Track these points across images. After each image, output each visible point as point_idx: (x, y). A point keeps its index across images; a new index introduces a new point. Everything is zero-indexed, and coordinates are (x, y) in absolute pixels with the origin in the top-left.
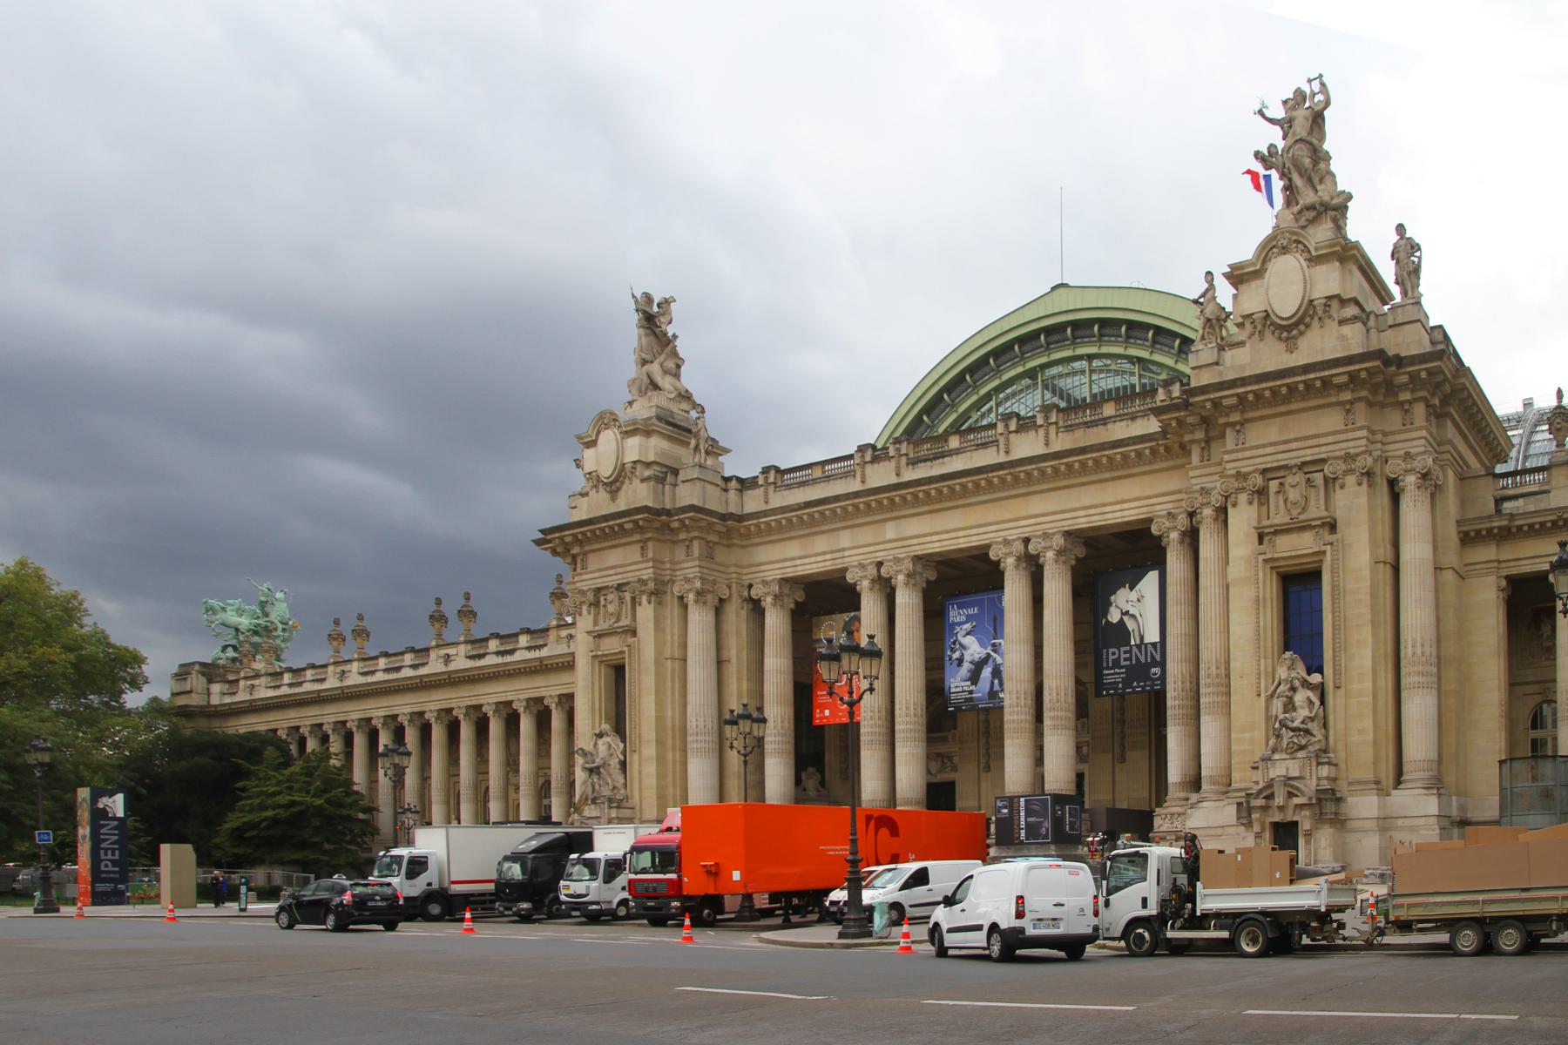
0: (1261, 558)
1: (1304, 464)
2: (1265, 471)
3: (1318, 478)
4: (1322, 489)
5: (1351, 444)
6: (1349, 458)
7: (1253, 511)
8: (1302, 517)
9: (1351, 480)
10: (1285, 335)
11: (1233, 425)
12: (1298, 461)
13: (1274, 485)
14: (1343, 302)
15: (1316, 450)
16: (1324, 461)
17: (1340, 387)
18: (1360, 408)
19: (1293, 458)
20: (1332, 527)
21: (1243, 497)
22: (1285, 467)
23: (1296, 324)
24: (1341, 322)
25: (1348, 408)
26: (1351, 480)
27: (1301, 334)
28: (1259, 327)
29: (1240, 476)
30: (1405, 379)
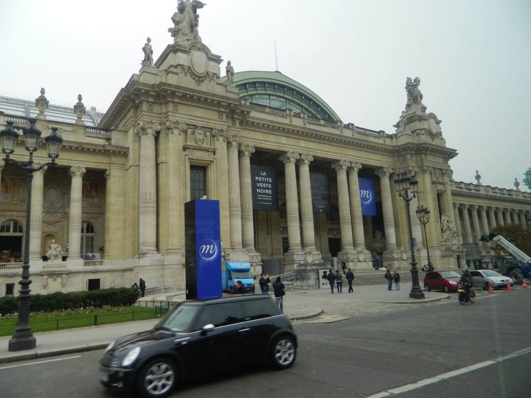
0: (187, 157)
1: (203, 127)
2: (187, 124)
3: (208, 134)
4: (209, 139)
5: (216, 125)
6: (222, 131)
7: (182, 137)
8: (203, 146)
9: (221, 139)
10: (197, 78)
11: (174, 103)
12: (200, 125)
13: (190, 131)
15: (207, 123)
16: (212, 129)
17: (223, 106)
18: (224, 116)
19: (199, 124)
20: (214, 153)
21: (176, 132)
22: (195, 126)
23: (201, 77)
25: (220, 113)
26: (221, 139)
27: (203, 81)
28: (186, 71)
29: (177, 123)
30: (239, 111)
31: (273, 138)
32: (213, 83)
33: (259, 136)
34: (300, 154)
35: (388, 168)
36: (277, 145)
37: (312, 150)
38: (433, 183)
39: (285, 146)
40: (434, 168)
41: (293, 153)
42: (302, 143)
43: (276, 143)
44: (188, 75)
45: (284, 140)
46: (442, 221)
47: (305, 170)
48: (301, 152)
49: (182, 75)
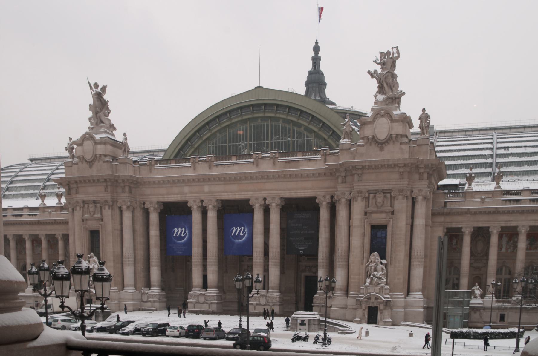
14: (105, 156)
24: (104, 162)
31: (176, 190)
32: (101, 162)
33: (163, 190)
34: (202, 201)
35: (324, 197)
36: (179, 196)
37: (217, 194)
38: (366, 213)
39: (187, 195)
40: (375, 192)
41: (195, 201)
42: (206, 189)
43: (177, 194)
44: (84, 161)
45: (186, 189)
46: (370, 261)
47: (212, 215)
48: (202, 198)
49: (80, 164)
